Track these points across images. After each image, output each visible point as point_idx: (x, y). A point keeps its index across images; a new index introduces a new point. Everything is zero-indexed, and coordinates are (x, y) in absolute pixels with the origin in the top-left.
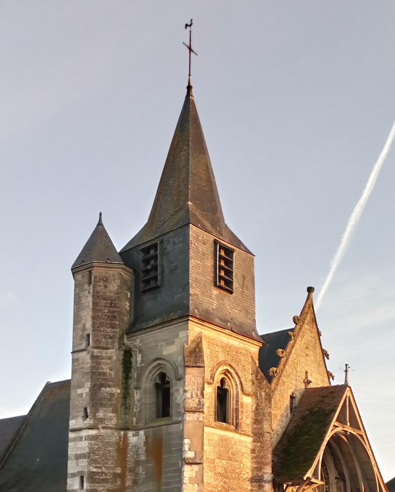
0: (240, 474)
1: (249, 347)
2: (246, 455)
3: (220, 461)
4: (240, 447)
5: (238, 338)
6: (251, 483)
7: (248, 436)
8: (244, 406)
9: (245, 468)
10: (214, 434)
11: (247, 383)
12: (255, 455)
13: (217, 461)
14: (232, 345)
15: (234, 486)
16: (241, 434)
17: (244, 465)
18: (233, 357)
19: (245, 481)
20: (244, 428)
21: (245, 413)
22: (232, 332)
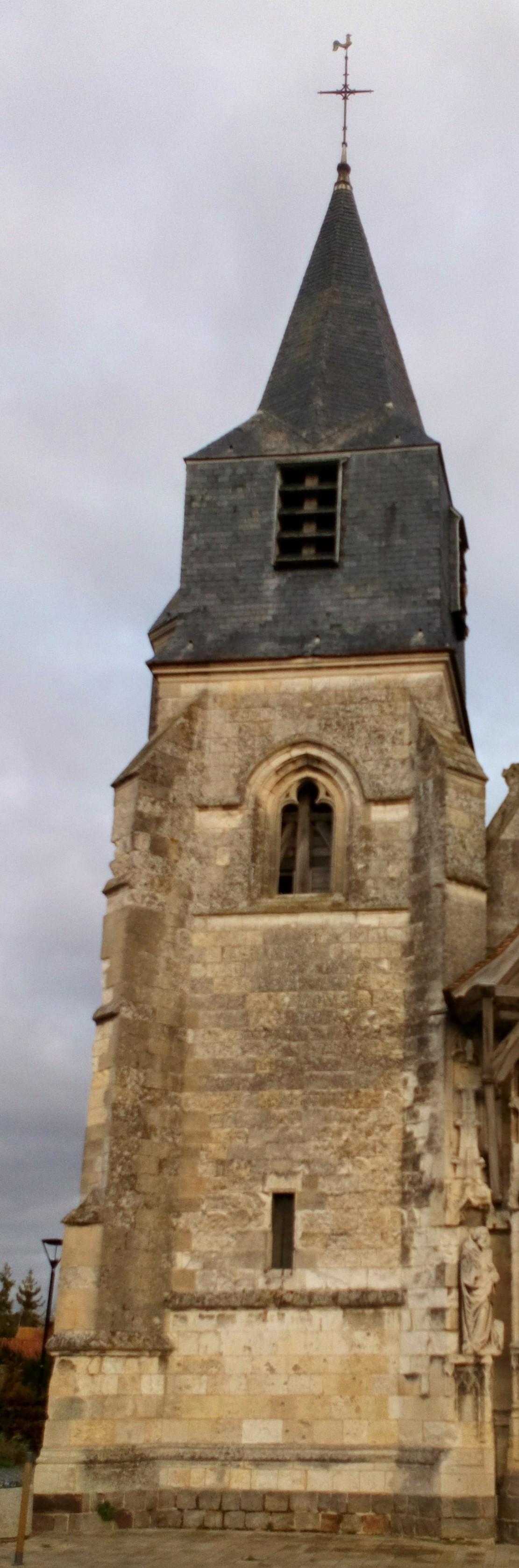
1: (401, 677)
2: (385, 965)
3: (270, 998)
4: (354, 946)
6: (405, 1037)
7: (392, 910)
8: (376, 834)
9: (375, 1000)
10: (244, 929)
11: (389, 771)
12: (412, 958)
13: (256, 998)
14: (325, 691)
15: (326, 1057)
17: (371, 992)
18: (328, 719)
19: (376, 1038)
20: (373, 891)
21: (379, 851)
22: (317, 660)
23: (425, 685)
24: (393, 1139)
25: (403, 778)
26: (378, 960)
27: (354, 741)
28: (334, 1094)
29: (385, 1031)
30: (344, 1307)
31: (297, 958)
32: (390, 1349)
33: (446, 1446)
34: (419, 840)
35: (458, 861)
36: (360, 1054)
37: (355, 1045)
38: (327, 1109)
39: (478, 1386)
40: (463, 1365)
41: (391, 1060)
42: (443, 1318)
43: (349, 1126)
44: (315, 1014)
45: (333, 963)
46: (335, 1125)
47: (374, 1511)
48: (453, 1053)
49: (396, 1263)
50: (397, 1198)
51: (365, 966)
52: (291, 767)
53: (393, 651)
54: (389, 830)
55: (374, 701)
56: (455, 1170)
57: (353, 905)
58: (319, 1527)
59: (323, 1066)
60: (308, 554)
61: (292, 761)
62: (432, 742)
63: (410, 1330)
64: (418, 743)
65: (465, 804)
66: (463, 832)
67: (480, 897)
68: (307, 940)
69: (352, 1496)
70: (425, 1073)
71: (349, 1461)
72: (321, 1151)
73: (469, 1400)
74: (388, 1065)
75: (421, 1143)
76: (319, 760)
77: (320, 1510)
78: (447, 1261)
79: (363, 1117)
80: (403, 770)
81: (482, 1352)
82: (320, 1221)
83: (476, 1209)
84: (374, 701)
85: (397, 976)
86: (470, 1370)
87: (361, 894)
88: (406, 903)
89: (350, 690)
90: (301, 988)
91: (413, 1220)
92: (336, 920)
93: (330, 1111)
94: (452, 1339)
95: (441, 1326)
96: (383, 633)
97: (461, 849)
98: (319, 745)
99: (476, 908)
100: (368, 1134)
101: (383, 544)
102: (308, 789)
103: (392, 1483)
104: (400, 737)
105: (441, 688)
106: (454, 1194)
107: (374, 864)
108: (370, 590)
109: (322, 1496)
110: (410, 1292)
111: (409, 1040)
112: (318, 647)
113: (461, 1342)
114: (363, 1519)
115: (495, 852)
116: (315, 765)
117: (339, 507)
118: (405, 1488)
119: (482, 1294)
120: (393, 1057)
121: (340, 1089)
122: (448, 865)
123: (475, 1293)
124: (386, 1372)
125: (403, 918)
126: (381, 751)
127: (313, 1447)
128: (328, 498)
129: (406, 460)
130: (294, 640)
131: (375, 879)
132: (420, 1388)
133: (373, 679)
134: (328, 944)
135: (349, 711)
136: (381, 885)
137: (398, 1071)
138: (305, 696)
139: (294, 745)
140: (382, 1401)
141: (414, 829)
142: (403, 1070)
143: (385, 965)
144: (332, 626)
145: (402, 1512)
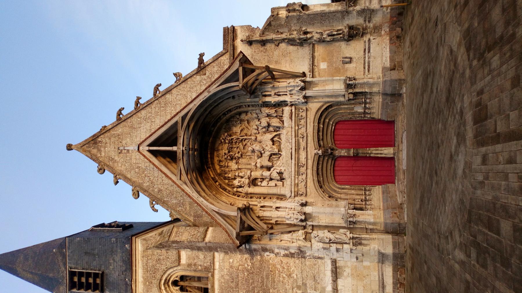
0: (248, 271)
1: (140, 252)
2: (231, 260)
5: (136, 270)
7: (214, 258)
8: (190, 262)
9: (242, 264)
11: (170, 257)
12: (229, 252)
14: (143, 278)
15: (260, 281)
16: (214, 269)
17: (240, 265)
18: (152, 277)
19: (254, 264)
20: (208, 263)
22: (133, 280)
23: (143, 245)
24: (285, 260)
25: (173, 253)
26: (229, 262)
27: (160, 268)
28: (272, 279)
29: (252, 262)
30: (337, 278)
31: (229, 289)
32: (349, 264)
33: (378, 250)
34: (192, 248)
35: (199, 237)
36: (259, 270)
37: (256, 271)
38: (276, 281)
39: (359, 239)
40: (353, 243)
41: (261, 260)
42: (339, 249)
43: (281, 274)
44: (246, 284)
45: (231, 277)
46: (281, 279)
47: (397, 272)
48: (258, 241)
49: (323, 261)
50: (303, 259)
51: (231, 267)
52: (168, 289)
53: (131, 255)
54: (189, 258)
55: (147, 261)
56: (294, 242)
57: (212, 270)
58: (403, 290)
59: (263, 282)
60: (98, 281)
61: (166, 289)
62: (161, 244)
63: (343, 258)
64: (161, 248)
65: (181, 234)
66: (190, 235)
67: (211, 229)
68: (223, 286)
69: (393, 279)
70: (265, 250)
71: (383, 279)
72: (289, 284)
73: (363, 242)
74: (262, 261)
75: (286, 252)
76: (166, 280)
77: (398, 289)
78: (322, 247)
79: (279, 269)
80: (170, 253)
81: (349, 237)
82: (311, 285)
83: (306, 236)
84: (147, 261)
85: (235, 257)
86: (354, 241)
87: (209, 267)
88: (212, 253)
89: (143, 269)
90: (238, 288)
91: (310, 255)
92: (217, 276)
93: (277, 280)
94: (345, 246)
95: (341, 249)
96: (125, 258)
97: (195, 236)
98: (161, 280)
99: (214, 231)
100: (284, 268)
101: (97, 256)
102: (175, 283)
103: (389, 266)
104: (159, 253)
105: (144, 239)
106: (302, 243)
107: (199, 263)
108: (112, 261)
109: (394, 288)
110: (332, 257)
111: (255, 254)
112: (129, 280)
113: (346, 243)
114: (400, 275)
115: (197, 224)
116: (167, 281)
117: (84, 271)
118: (390, 262)
119: (332, 236)
120: (260, 260)
121: (270, 277)
122: (200, 241)
123: (331, 239)
124: (356, 266)
125: (216, 254)
126: (163, 260)
127: (379, 290)
128: (81, 274)
129: (71, 248)
130: (126, 287)
131: (204, 263)
132: (360, 256)
133: (140, 262)
134: (224, 279)
135: (150, 270)
136: (206, 261)
137: (264, 257)
138: (145, 284)
139: (160, 288)
140: (365, 267)
141: (189, 250)
142: (264, 256)
143: (231, 260)
144: (123, 274)
145: (398, 263)
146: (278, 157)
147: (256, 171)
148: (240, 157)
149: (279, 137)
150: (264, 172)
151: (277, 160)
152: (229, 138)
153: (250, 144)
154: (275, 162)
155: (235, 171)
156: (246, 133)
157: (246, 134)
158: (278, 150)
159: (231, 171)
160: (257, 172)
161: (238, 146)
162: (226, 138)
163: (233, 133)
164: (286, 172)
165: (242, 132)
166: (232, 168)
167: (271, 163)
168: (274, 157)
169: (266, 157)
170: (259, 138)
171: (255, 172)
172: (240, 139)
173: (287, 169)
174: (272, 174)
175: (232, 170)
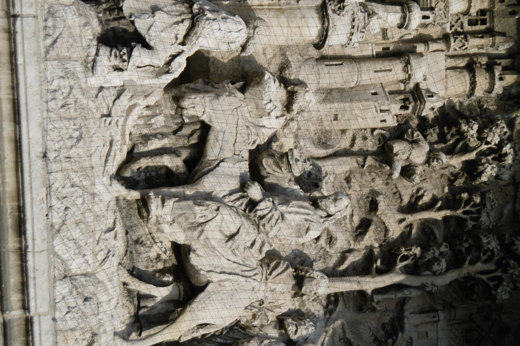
146: (144, 163)
147: (282, 50)
148: (390, 139)
149: (139, 308)
150: (236, 46)
151: (146, 138)
152: (480, 266)
153: (331, 240)
154: (159, 122)
155: (425, 40)
156: (360, 317)
157: (360, 309)
158: (148, 211)
159: (445, 38)
160: (282, 41)
161: (410, 218)
162: (499, 264)
163: (448, 307)
164: (78, 54)
165: (387, 319)
166: (441, 56)
167: (189, 112)
168: (167, 161)
169: (228, 154)
170: (279, 288)
171: (297, 39)
172: (400, 265)
173: (73, 75)
174: (183, 29)
175: (440, 46)
